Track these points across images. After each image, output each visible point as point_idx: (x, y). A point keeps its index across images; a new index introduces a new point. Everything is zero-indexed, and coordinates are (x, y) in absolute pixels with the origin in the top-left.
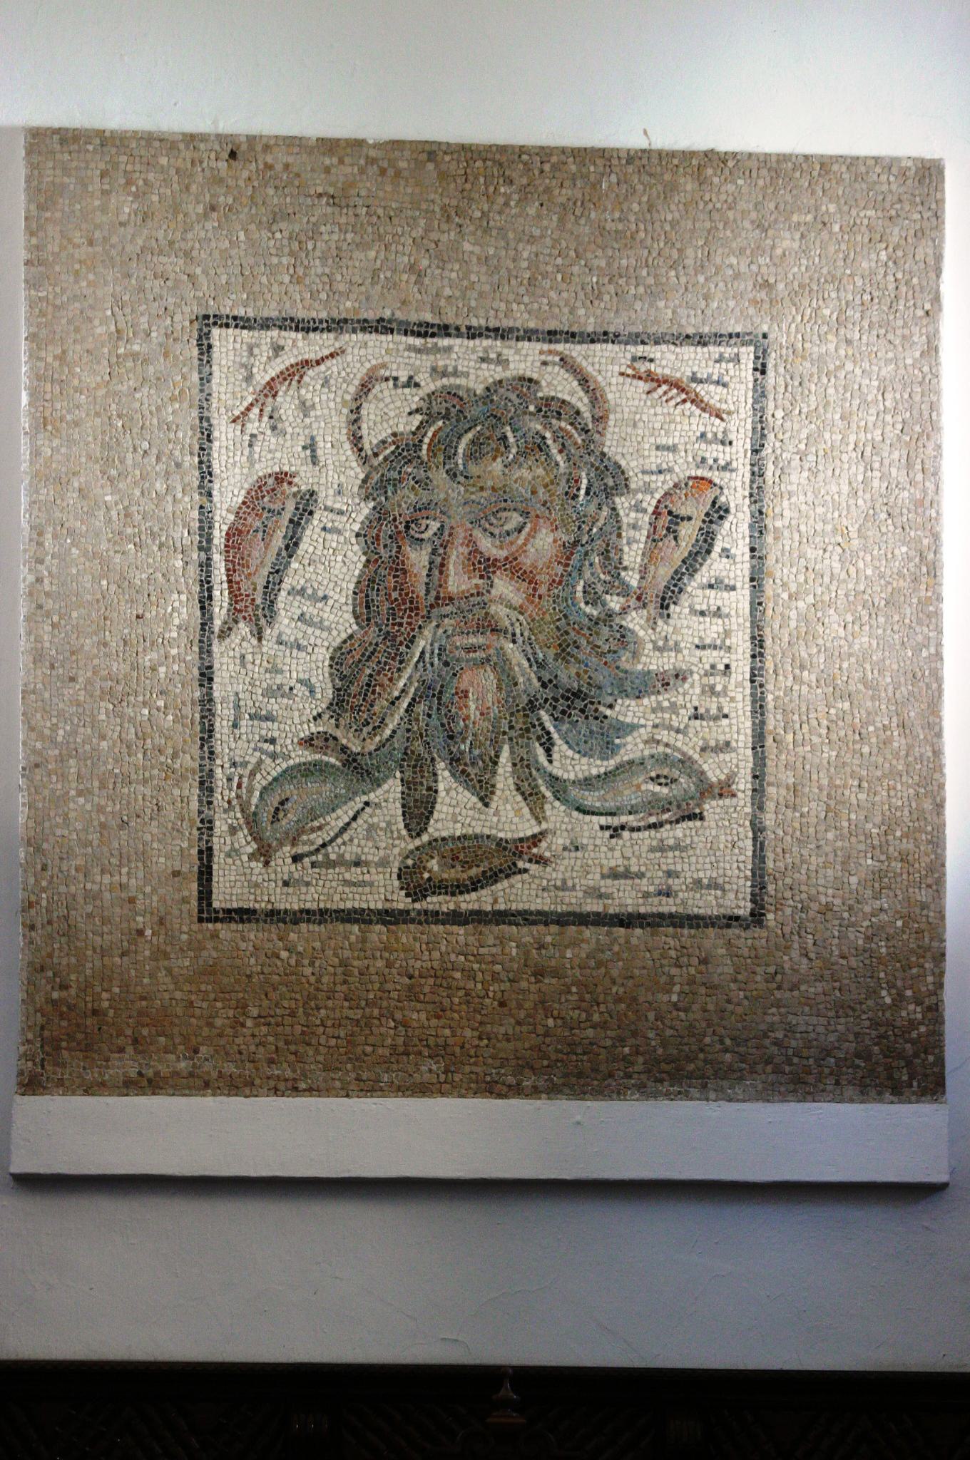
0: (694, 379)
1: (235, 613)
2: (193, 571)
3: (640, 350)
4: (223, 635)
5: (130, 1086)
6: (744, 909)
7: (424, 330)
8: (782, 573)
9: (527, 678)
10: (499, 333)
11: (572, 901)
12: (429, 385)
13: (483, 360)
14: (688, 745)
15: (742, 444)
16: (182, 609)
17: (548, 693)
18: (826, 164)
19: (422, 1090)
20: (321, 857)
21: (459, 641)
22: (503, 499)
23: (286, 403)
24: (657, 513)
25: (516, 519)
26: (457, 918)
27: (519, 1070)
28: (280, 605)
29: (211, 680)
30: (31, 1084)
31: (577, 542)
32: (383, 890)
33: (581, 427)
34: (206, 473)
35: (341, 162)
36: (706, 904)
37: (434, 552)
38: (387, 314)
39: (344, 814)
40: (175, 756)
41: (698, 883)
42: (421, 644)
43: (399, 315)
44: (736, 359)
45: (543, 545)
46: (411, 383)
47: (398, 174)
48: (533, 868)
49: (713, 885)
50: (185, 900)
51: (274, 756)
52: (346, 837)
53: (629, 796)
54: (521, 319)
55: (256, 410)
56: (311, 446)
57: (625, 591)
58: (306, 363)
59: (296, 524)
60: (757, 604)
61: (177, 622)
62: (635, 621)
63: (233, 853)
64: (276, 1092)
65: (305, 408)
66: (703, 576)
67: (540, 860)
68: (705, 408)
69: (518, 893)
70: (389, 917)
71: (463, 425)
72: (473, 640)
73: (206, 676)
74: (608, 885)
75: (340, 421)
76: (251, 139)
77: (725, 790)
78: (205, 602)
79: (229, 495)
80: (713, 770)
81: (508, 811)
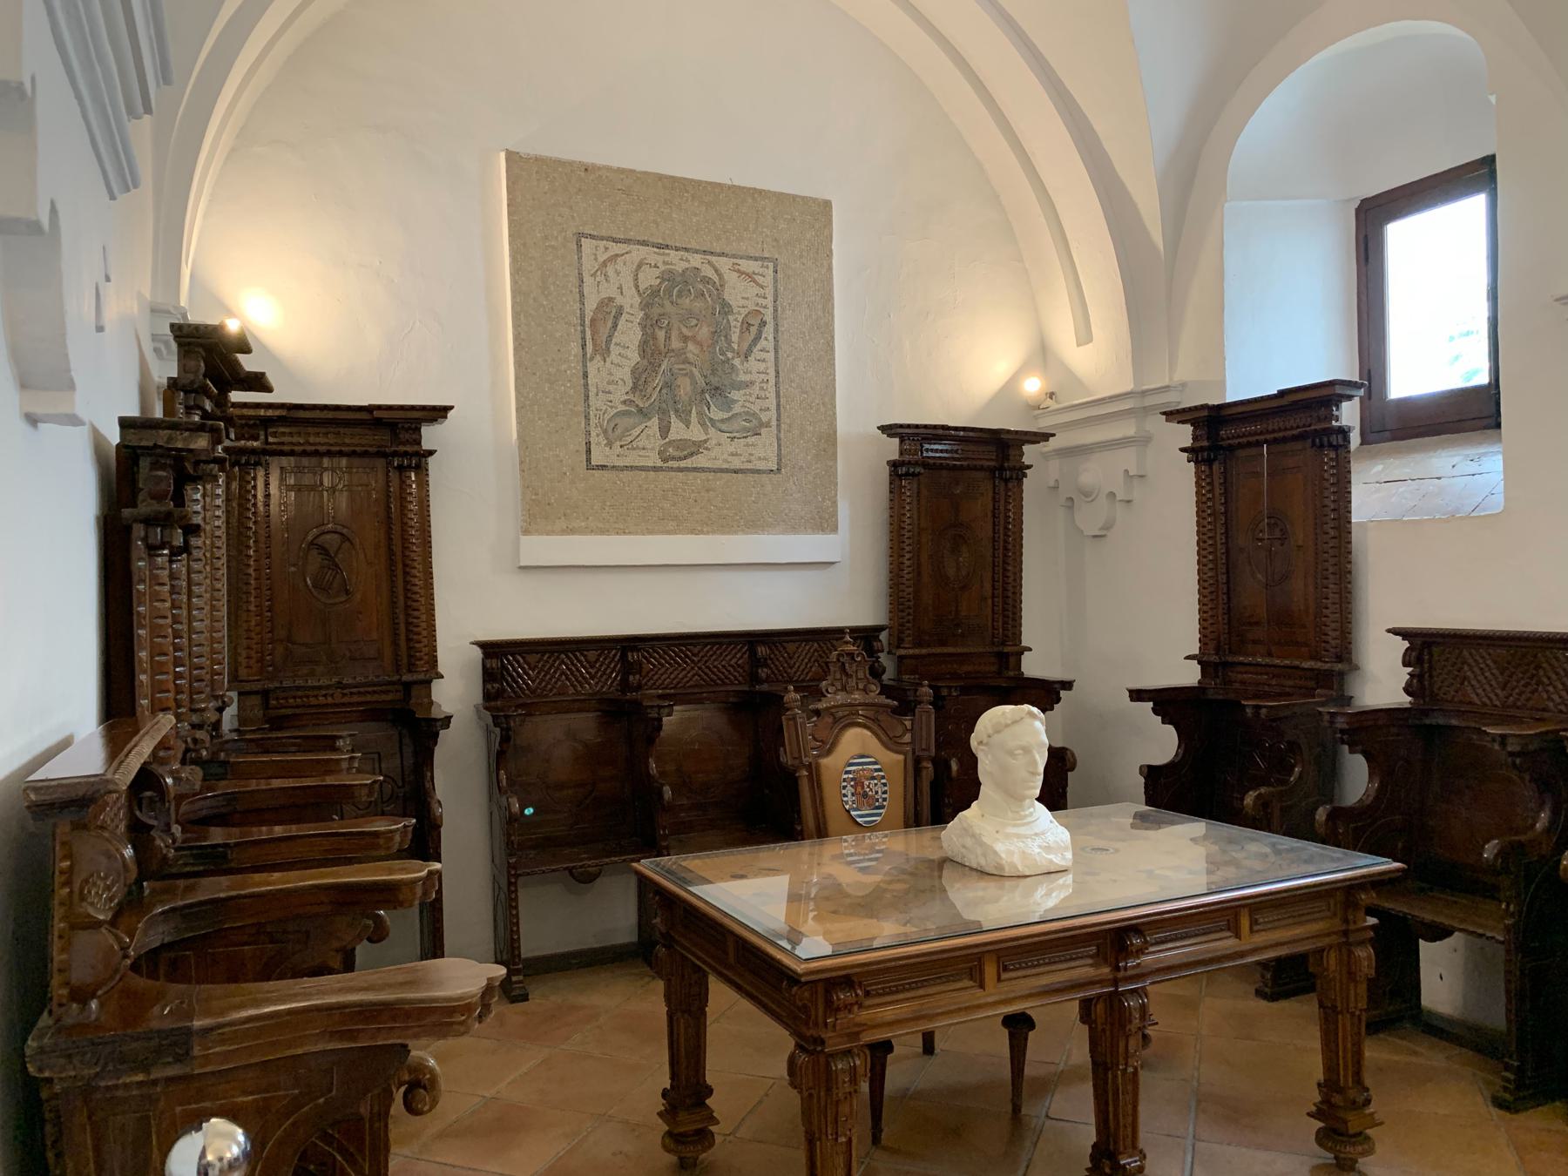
1: (595, 351)
4: (592, 359)
7: (660, 246)
8: (784, 348)
9: (701, 381)
10: (686, 250)
11: (719, 464)
12: (662, 268)
14: (755, 408)
15: (770, 298)
16: (575, 348)
18: (794, 197)
19: (668, 533)
22: (691, 314)
23: (610, 270)
25: (694, 322)
26: (680, 470)
30: (526, 532)
36: (761, 465)
45: (704, 332)
53: (735, 426)
54: (693, 245)
56: (620, 288)
59: (617, 318)
60: (776, 358)
62: (737, 362)
63: (598, 444)
65: (618, 273)
66: (759, 347)
69: (700, 461)
70: (655, 469)
71: (676, 284)
73: (585, 375)
75: (631, 279)
77: (768, 425)
78: (584, 346)
79: (591, 305)
80: (764, 417)
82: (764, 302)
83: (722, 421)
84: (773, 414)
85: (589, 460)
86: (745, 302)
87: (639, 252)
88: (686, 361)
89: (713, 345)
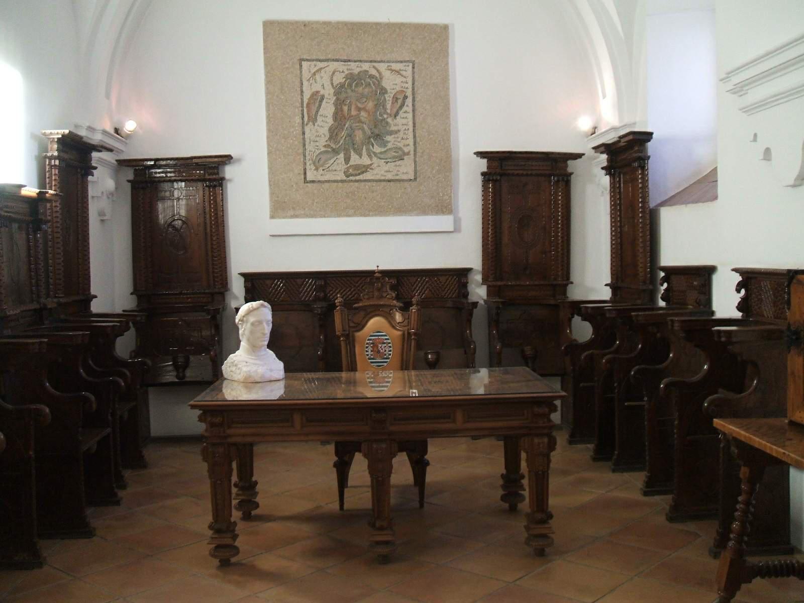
0: (400, 70)
2: (300, 112)
3: (389, 64)
4: (307, 125)
5: (292, 217)
6: (412, 178)
7: (345, 61)
8: (419, 110)
9: (369, 132)
10: (361, 61)
11: (378, 177)
12: (347, 72)
13: (357, 67)
14: (400, 145)
16: (298, 119)
17: (373, 135)
20: (328, 169)
21: (354, 125)
22: (362, 96)
23: (317, 77)
24: (393, 97)
25: (365, 100)
27: (369, 211)
28: (318, 118)
29: (304, 134)
31: (377, 104)
32: (341, 176)
33: (377, 81)
34: (302, 92)
35: (327, 26)
36: (405, 177)
37: (349, 107)
38: (337, 58)
39: (332, 161)
40: (298, 149)
41: (403, 173)
42: (347, 126)
43: (340, 58)
44: (408, 66)
45: (370, 105)
46: (343, 72)
47: (339, 28)
48: (371, 171)
49: (406, 173)
50: (301, 179)
51: (318, 149)
52: (333, 165)
53: (389, 156)
54: (365, 58)
55: (311, 78)
56: (323, 85)
57: (388, 114)
58: (321, 69)
59: (321, 101)
60: (414, 116)
61: (297, 122)
62: (389, 120)
63: (311, 169)
64: (321, 217)
65: (322, 78)
67: (372, 169)
68: (402, 76)
70: (342, 181)
71: (354, 79)
72: (357, 124)
73: (304, 133)
74: (385, 174)
76: (309, 22)
77: (408, 154)
78: (303, 118)
80: (406, 150)
81: (365, 159)
82: (406, 85)
83: (381, 153)
84: (411, 148)
85: (305, 178)
86: (395, 87)
87: (333, 66)
88: (360, 121)
89: (376, 112)
